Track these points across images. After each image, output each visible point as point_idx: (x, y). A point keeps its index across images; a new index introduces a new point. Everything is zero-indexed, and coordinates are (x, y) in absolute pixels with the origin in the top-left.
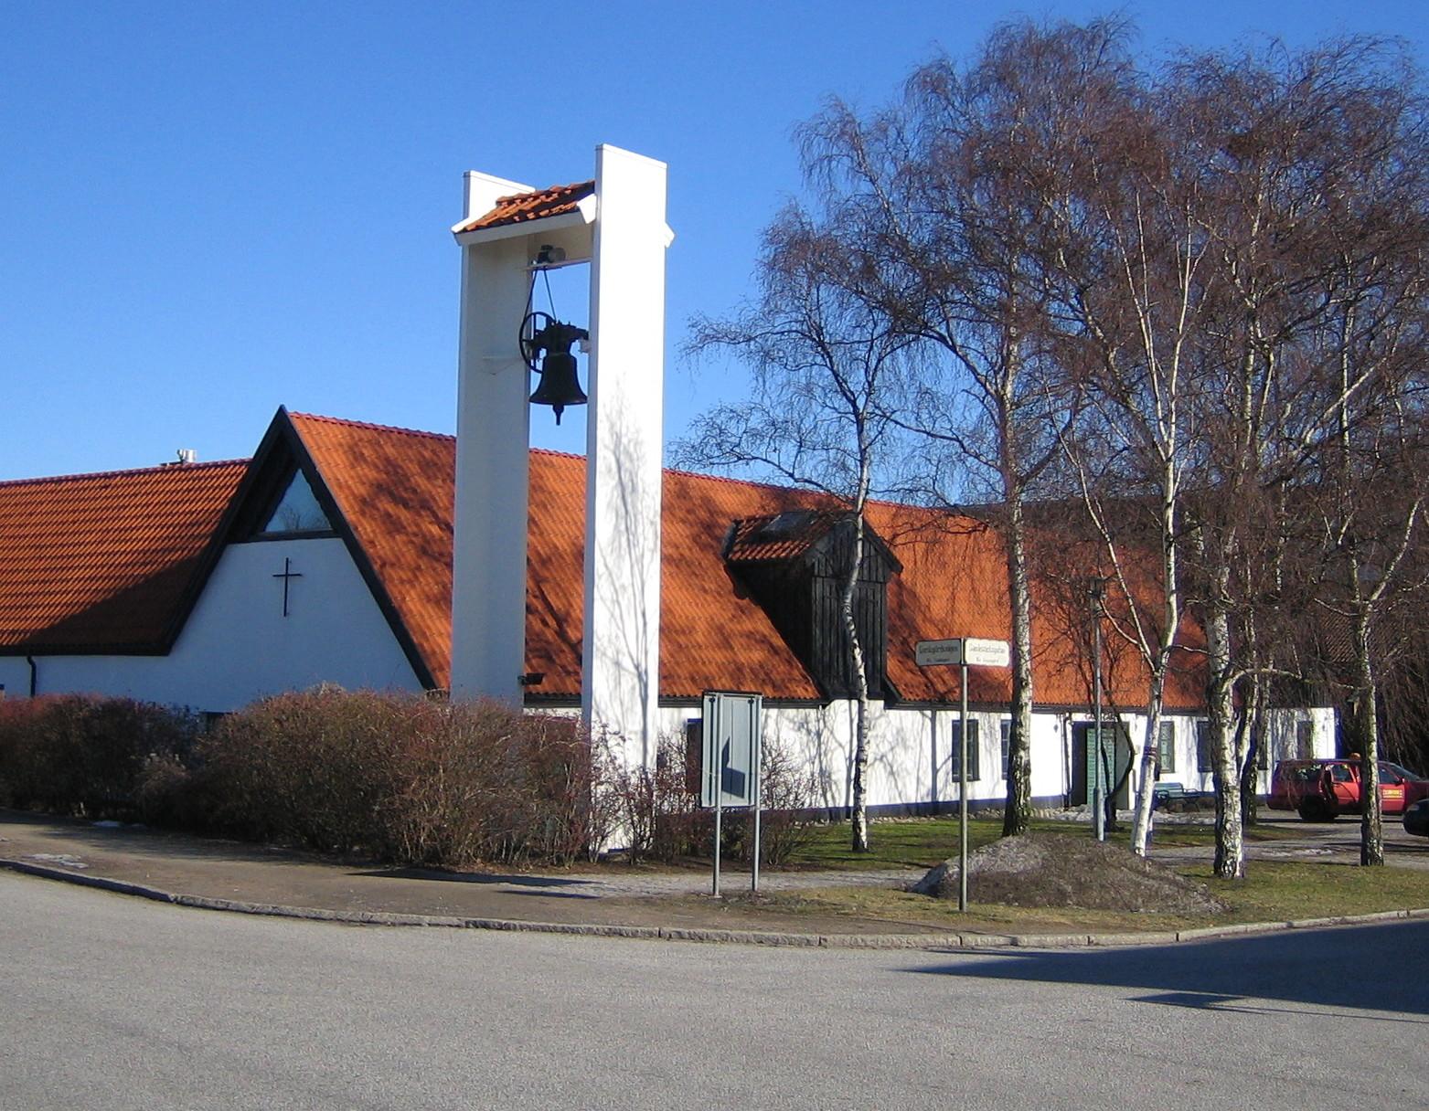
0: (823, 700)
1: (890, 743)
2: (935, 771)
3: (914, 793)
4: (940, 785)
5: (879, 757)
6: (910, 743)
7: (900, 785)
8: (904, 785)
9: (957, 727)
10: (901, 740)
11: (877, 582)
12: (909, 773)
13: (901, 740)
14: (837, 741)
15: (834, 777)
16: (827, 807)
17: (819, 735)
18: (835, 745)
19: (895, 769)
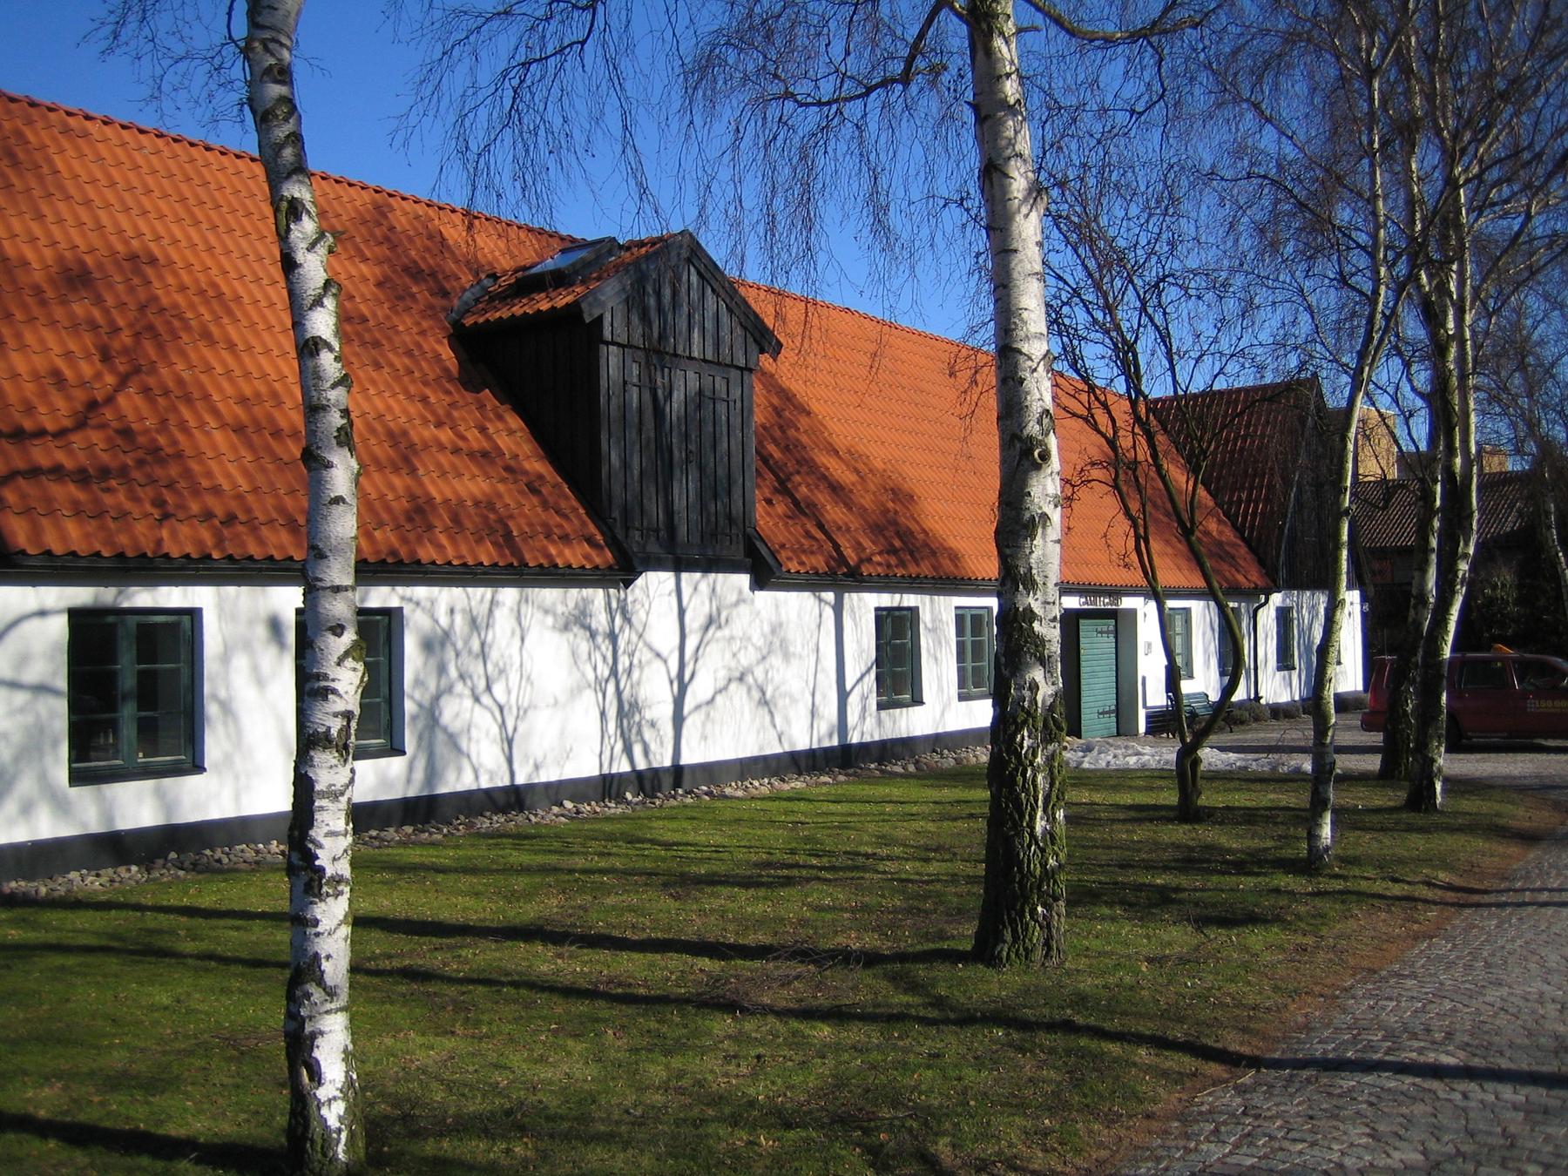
0: (622, 572)
1: (758, 649)
2: (843, 696)
3: (803, 733)
4: (853, 717)
5: (737, 674)
6: (796, 647)
7: (778, 720)
8: (787, 721)
9: (882, 615)
10: (777, 642)
11: (732, 366)
12: (794, 700)
13: (777, 642)
14: (651, 649)
15: (648, 715)
16: (634, 770)
17: (613, 637)
18: (646, 655)
19: (769, 695)
